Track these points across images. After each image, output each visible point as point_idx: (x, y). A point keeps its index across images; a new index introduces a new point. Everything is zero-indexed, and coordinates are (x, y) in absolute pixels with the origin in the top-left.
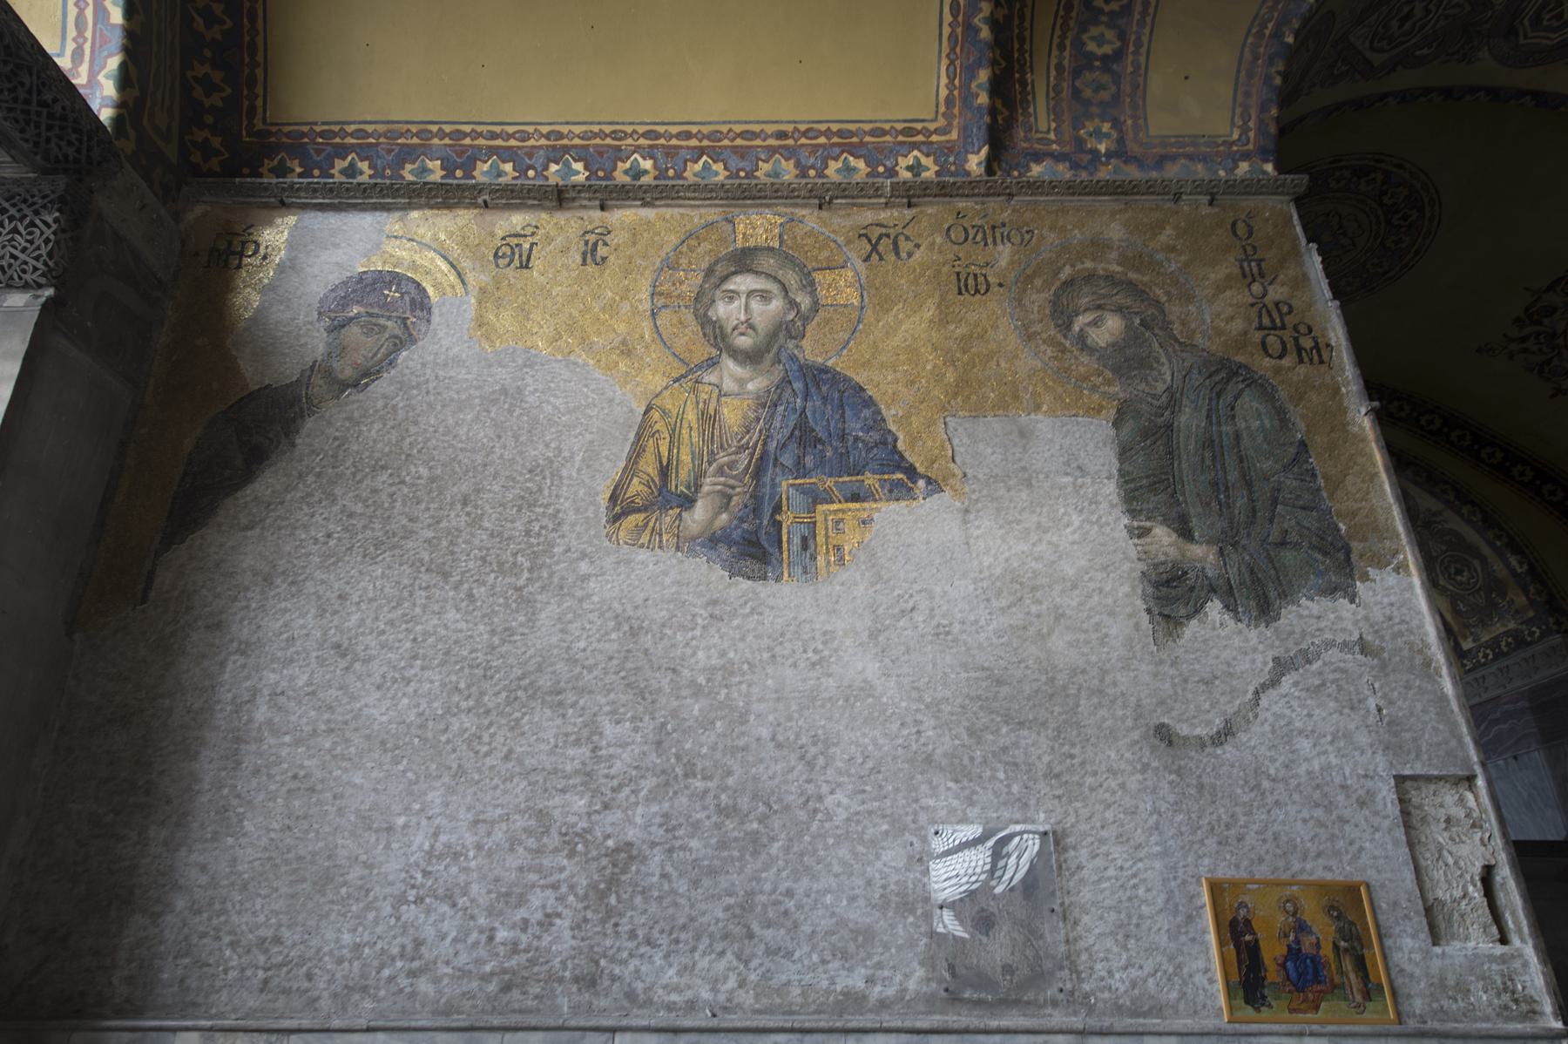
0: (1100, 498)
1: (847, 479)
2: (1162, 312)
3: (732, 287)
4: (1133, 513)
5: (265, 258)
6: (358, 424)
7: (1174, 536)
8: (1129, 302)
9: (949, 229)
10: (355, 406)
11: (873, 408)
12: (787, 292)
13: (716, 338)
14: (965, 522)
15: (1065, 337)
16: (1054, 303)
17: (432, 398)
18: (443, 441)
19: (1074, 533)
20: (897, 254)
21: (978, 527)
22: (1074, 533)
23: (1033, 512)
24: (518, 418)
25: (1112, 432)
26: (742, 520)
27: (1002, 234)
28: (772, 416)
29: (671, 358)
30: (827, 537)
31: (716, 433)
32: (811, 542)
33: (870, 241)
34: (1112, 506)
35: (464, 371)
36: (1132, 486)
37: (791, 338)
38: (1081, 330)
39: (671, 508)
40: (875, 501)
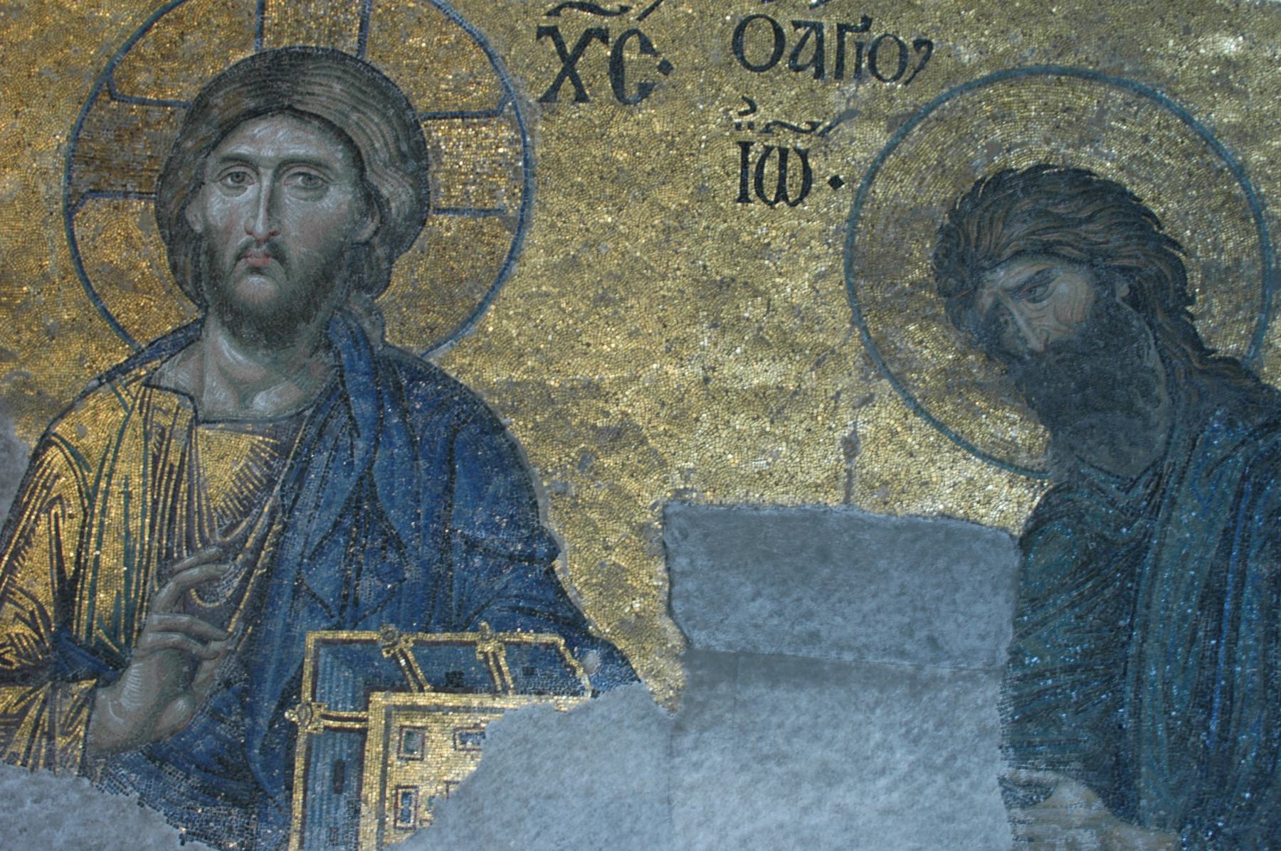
0: (962, 715)
1: (443, 637)
2: (1180, 270)
3: (244, 150)
4: (1022, 749)
7: (1098, 803)
8: (1115, 240)
9: (740, 31)
11: (515, 476)
12: (362, 170)
13: (197, 279)
14: (671, 753)
15: (957, 322)
16: (946, 233)
19: (889, 790)
20: (618, 85)
21: (697, 766)
22: (889, 790)
23: (817, 738)
25: (1015, 560)
26: (216, 716)
27: (859, 47)
28: (300, 475)
29: (98, 322)
30: (385, 764)
31: (181, 511)
32: (352, 773)
33: (560, 45)
34: (984, 732)
36: (1036, 688)
37: (362, 287)
38: (997, 305)
39: (76, 679)
40: (494, 693)
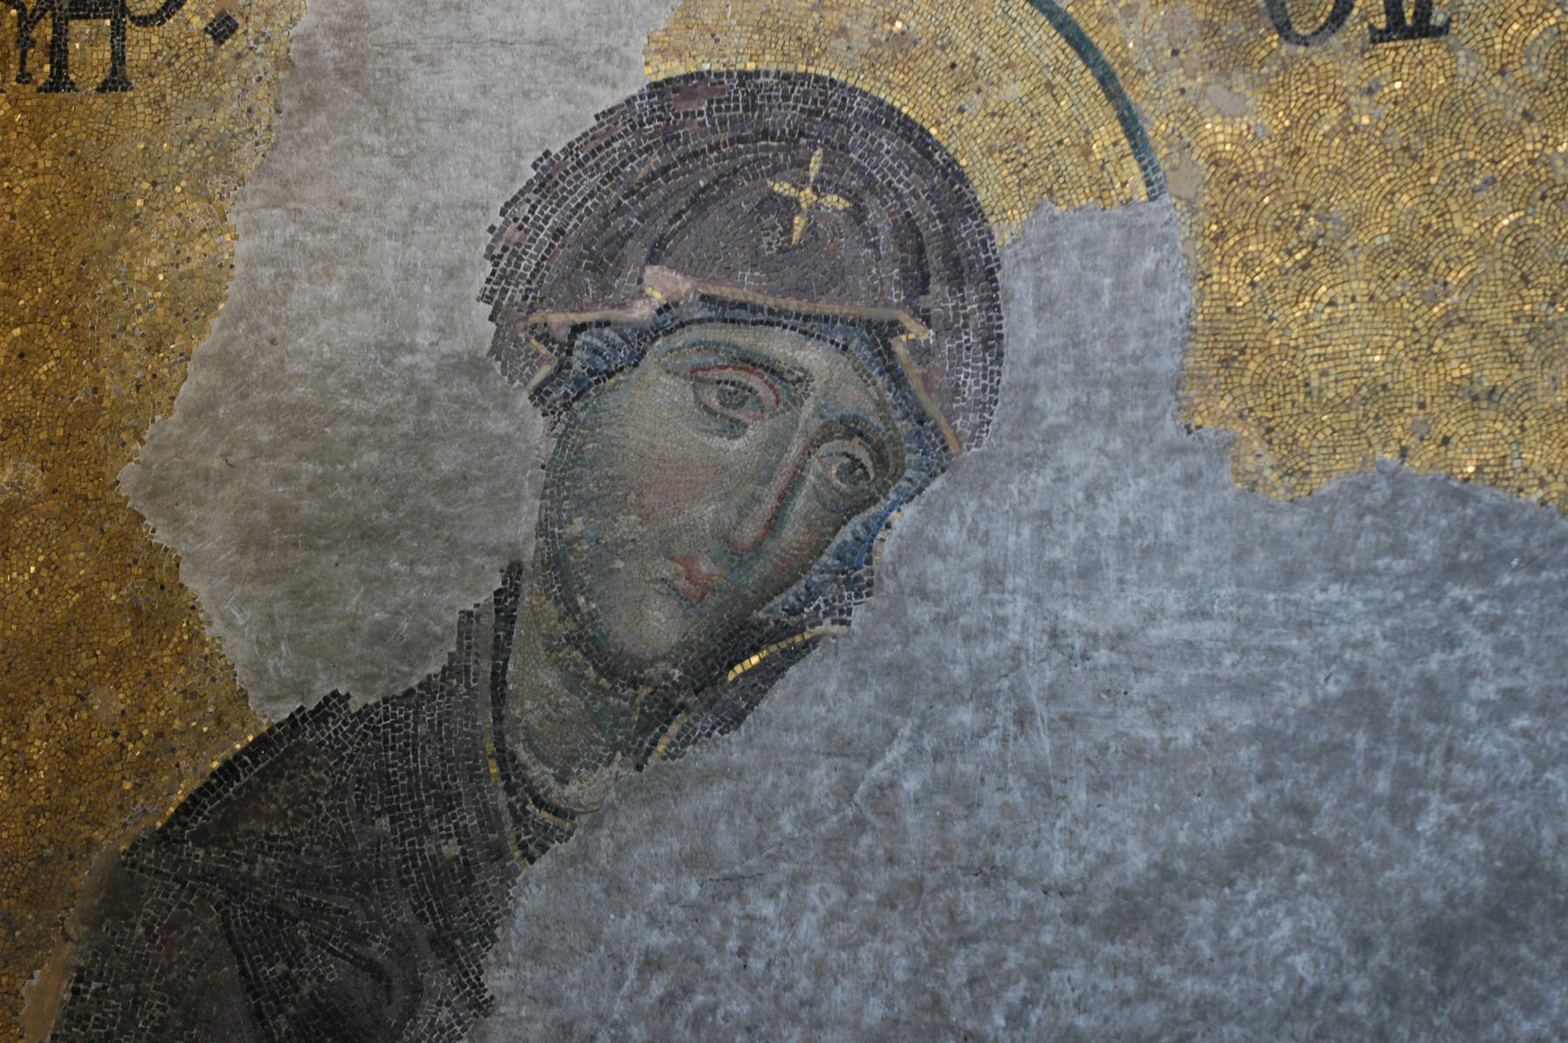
5: (222, 28)
6: (736, 884)
10: (716, 796)
17: (1045, 743)
18: (1115, 967)
24: (1440, 843)
35: (1174, 601)
